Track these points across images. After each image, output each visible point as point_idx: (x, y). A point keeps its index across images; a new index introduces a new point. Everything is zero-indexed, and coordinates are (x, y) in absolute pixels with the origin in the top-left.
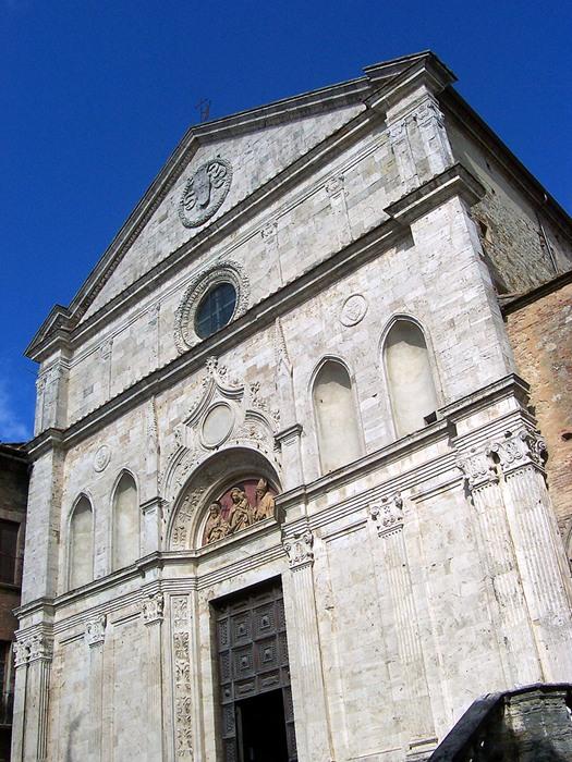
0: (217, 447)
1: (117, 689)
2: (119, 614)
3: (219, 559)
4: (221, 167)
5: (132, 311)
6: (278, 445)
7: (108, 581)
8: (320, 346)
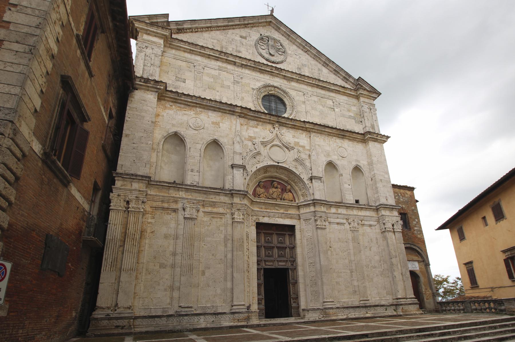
0: (278, 163)
1: (205, 247)
2: (209, 209)
3: (263, 207)
4: (281, 47)
5: (225, 65)
6: (311, 179)
7: (204, 189)
8: (328, 155)
